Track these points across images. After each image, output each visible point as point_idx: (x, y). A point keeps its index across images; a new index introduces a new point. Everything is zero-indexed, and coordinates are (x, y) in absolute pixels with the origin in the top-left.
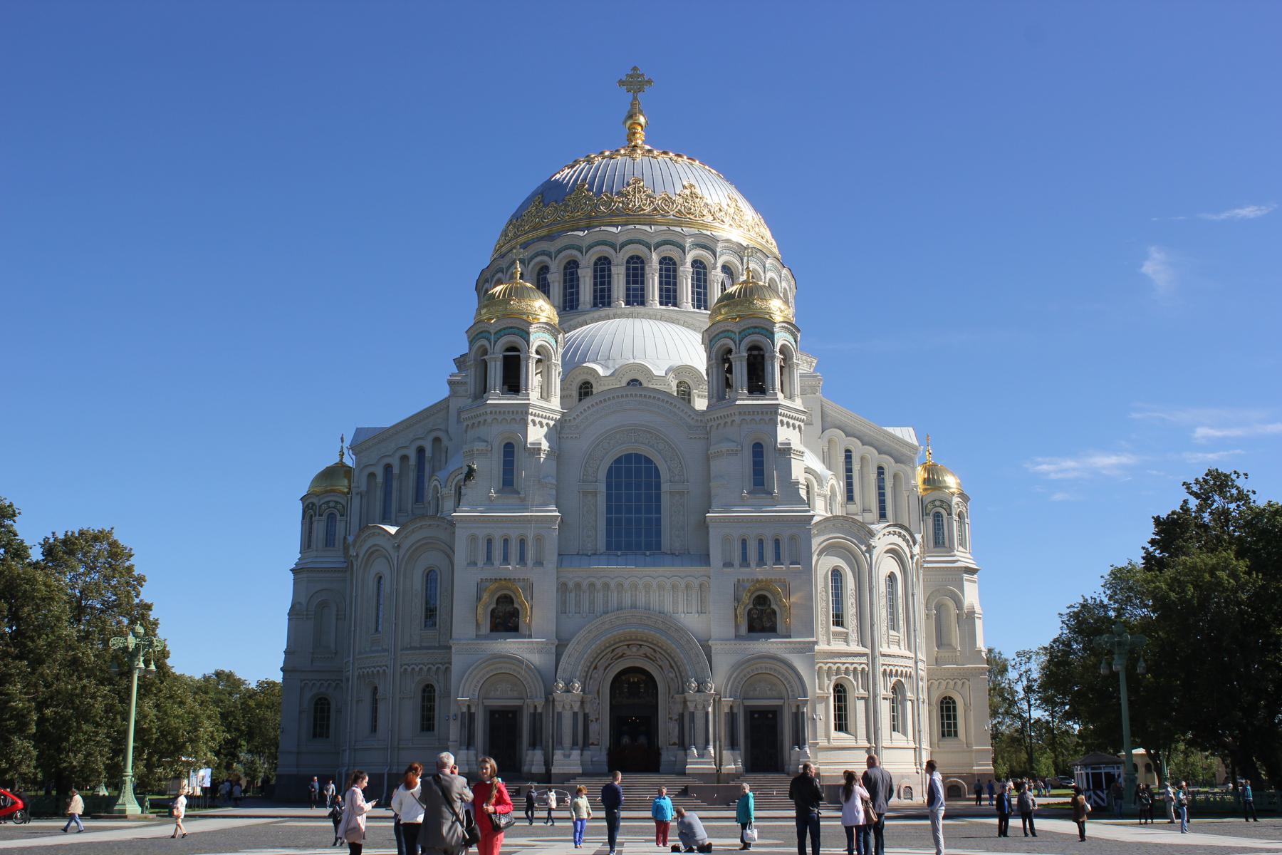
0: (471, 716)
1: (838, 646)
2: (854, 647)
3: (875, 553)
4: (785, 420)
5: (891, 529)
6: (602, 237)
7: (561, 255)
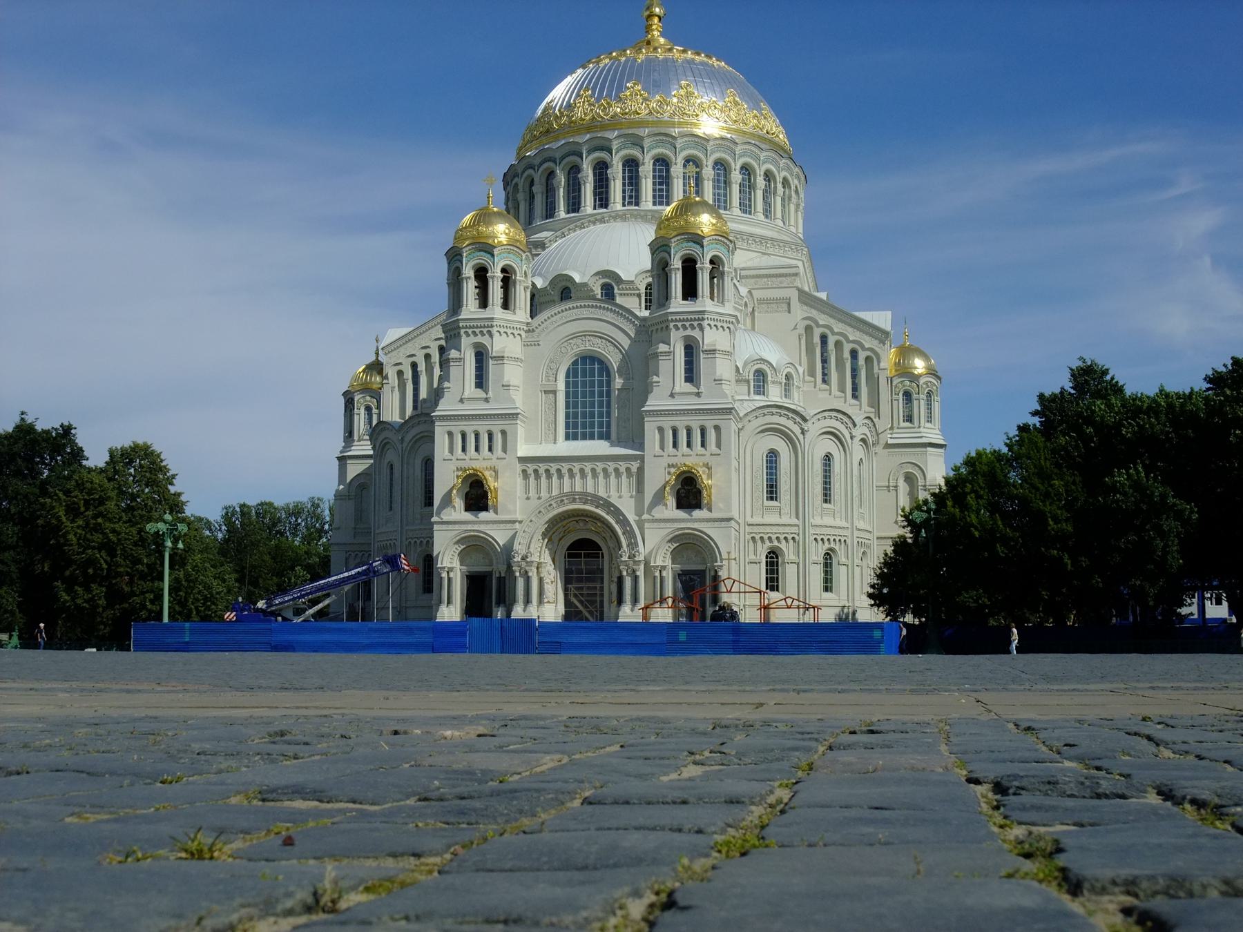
0: (449, 579)
1: (772, 518)
2: (785, 519)
3: (807, 435)
4: (712, 323)
5: (826, 414)
6: (597, 143)
7: (564, 162)
